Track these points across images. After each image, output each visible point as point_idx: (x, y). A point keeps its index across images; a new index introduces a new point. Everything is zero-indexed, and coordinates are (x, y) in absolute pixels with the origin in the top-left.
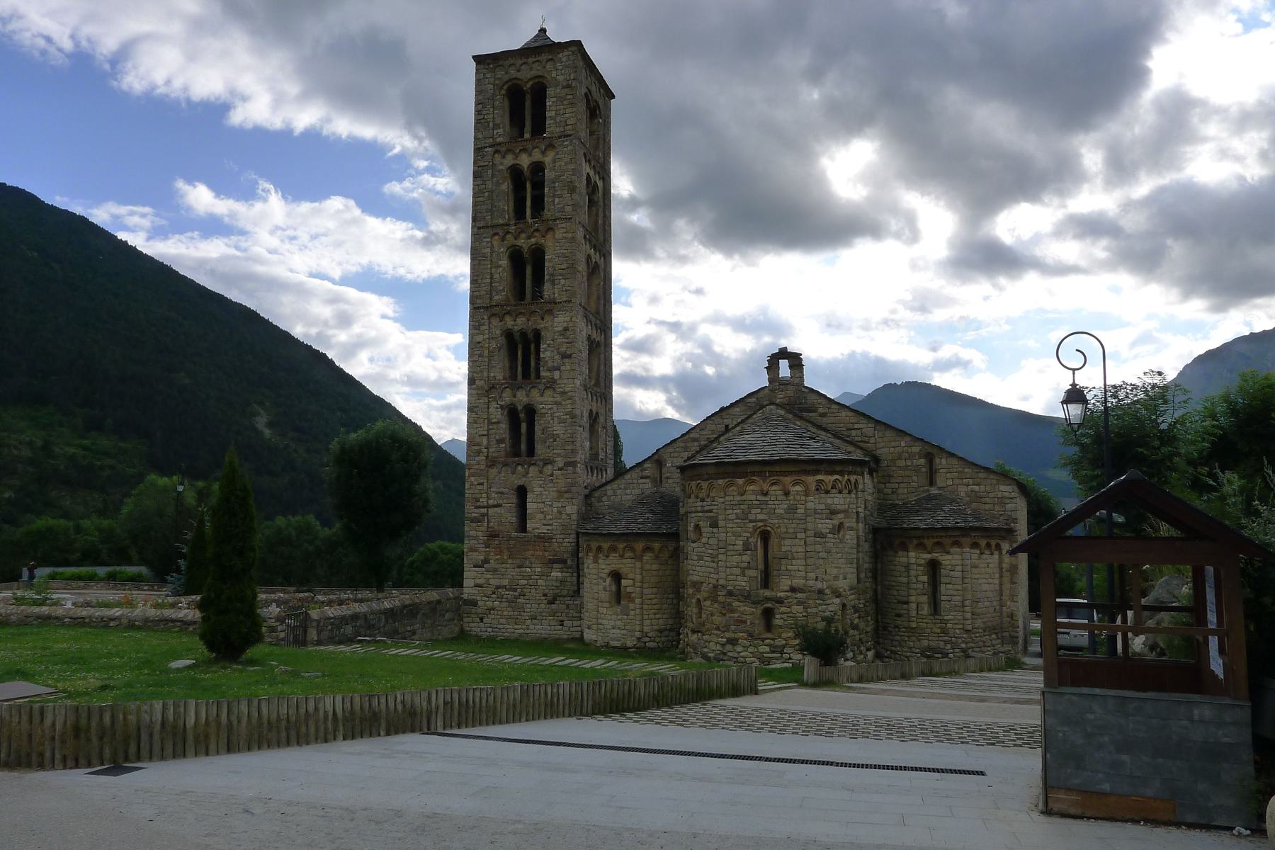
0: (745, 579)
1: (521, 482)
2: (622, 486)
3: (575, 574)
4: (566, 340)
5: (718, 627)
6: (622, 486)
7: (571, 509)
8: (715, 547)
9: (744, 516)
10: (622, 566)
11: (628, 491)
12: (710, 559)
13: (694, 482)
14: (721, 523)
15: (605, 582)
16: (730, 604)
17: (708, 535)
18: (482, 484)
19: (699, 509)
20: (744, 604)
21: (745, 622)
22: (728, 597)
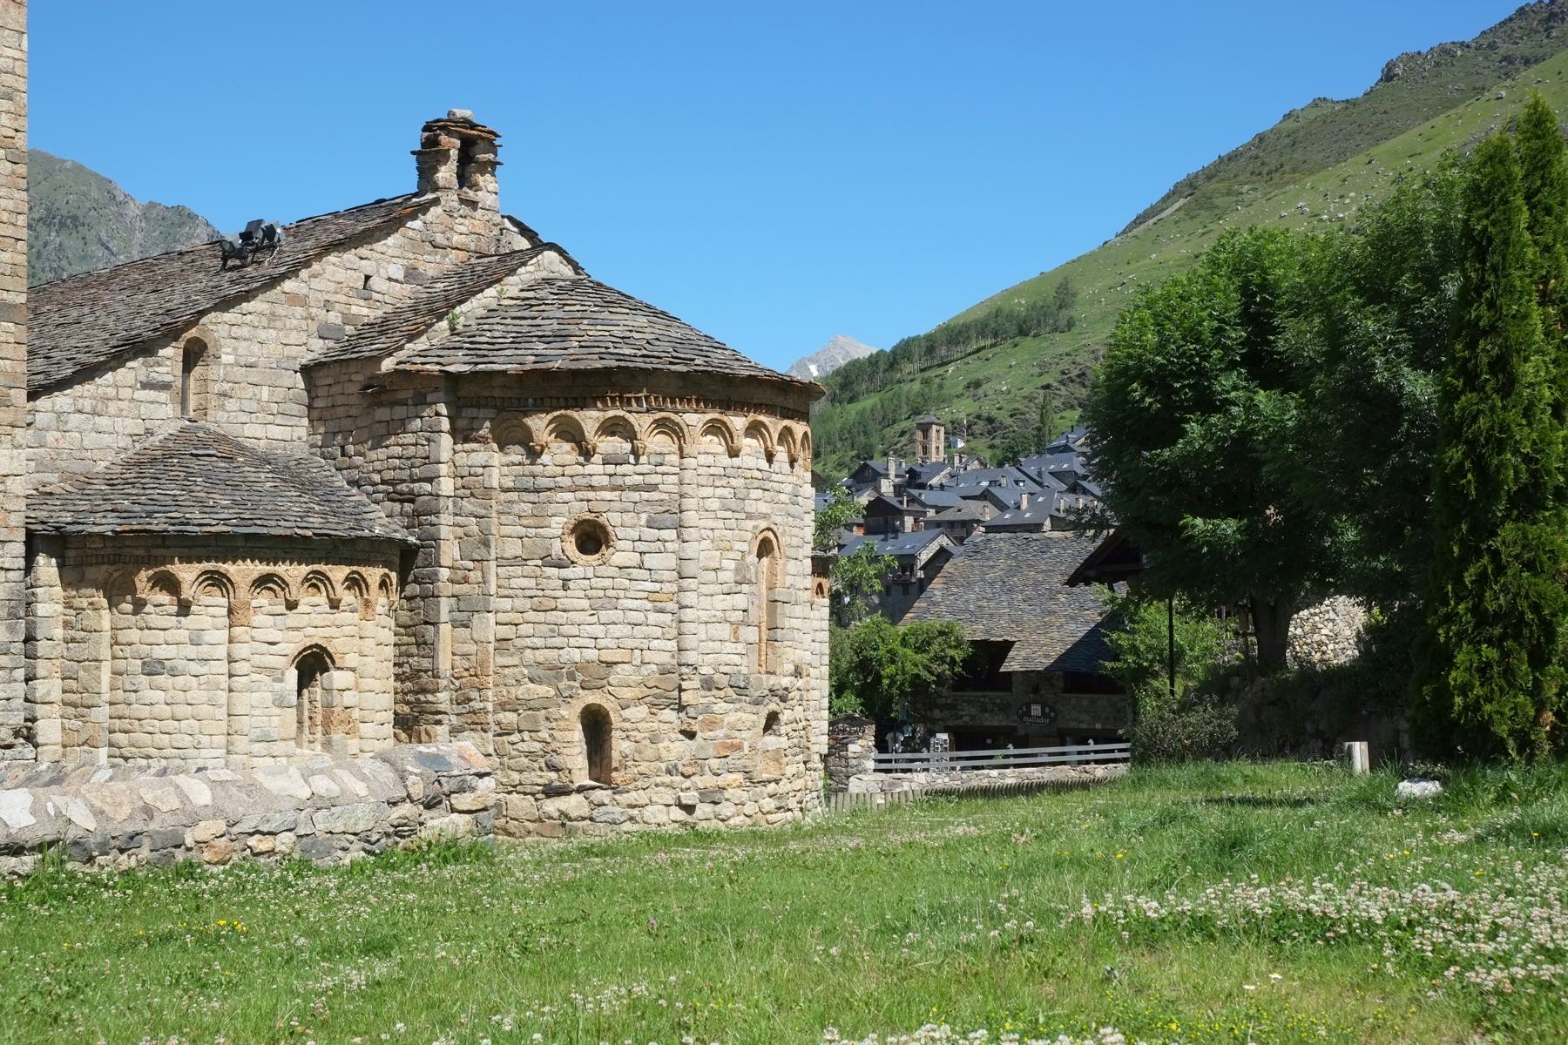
0: (740, 648)
2: (87, 405)
3: (20, 674)
5: (675, 766)
6: (87, 405)
8: (667, 575)
9: (736, 507)
10: (332, 631)
11: (103, 422)
12: (649, 605)
13: (594, 413)
14: (690, 517)
15: (281, 680)
16: (707, 710)
17: (642, 546)
19: (605, 481)
20: (738, 706)
21: (739, 748)
22: (703, 693)
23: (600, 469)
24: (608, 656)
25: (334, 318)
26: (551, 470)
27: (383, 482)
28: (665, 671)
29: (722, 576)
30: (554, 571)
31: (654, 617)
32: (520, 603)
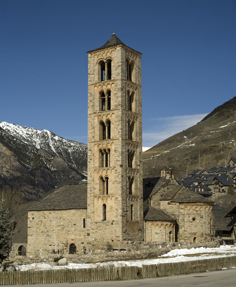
1: (132, 203)
4: (140, 157)
7: (142, 213)
14: (204, 217)
16: (206, 237)
17: (200, 220)
18: (125, 203)
19: (196, 213)
23: (195, 212)
24: (196, 232)
25: (162, 194)
26: (190, 212)
27: (171, 213)
28: (202, 233)
29: (207, 223)
30: (190, 223)
31: (201, 228)
32: (187, 226)
